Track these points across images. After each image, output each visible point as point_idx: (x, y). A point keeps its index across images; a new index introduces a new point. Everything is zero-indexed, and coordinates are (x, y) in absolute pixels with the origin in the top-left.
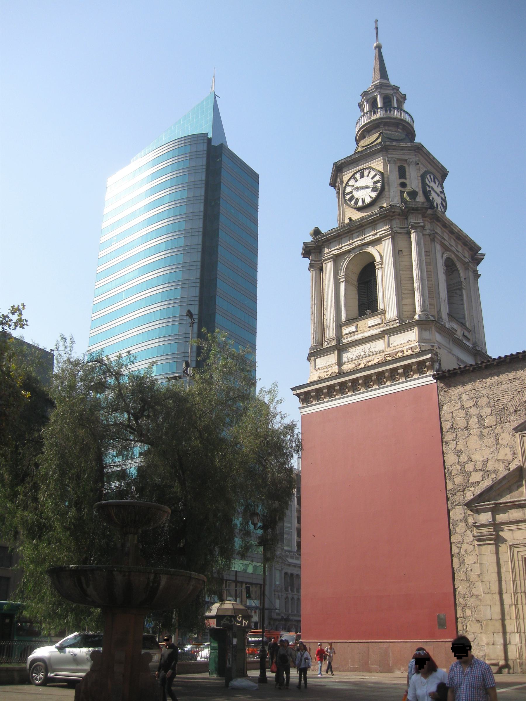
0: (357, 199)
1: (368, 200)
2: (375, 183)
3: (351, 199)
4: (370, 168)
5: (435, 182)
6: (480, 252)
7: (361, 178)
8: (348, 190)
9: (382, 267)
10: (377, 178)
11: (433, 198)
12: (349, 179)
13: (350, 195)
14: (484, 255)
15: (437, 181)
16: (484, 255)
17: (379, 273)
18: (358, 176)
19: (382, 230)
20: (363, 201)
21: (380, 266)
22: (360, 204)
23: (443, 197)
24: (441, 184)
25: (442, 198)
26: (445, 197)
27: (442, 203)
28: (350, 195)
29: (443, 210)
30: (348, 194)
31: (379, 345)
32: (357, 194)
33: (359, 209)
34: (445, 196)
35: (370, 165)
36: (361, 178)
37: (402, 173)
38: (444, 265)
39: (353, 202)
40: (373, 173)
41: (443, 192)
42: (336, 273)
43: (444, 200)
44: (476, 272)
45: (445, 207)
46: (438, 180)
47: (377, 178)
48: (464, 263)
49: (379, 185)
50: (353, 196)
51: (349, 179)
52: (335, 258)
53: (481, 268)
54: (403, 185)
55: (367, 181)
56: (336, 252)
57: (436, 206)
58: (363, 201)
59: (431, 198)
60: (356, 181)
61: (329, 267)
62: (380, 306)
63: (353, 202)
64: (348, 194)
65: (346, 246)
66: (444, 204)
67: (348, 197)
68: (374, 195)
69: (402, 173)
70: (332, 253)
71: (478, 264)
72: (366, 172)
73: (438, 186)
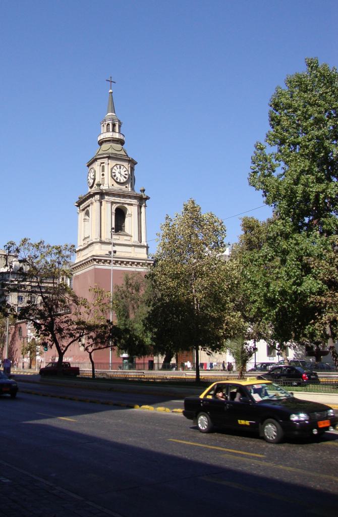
1: (122, 181)
2: (126, 174)
8: (113, 171)
18: (118, 166)
22: (118, 181)
30: (113, 173)
33: (117, 182)
39: (115, 178)
40: (125, 169)
47: (126, 173)
56: (113, 200)
63: (115, 178)
65: (117, 200)
67: (113, 174)
68: (125, 180)
72: (122, 167)
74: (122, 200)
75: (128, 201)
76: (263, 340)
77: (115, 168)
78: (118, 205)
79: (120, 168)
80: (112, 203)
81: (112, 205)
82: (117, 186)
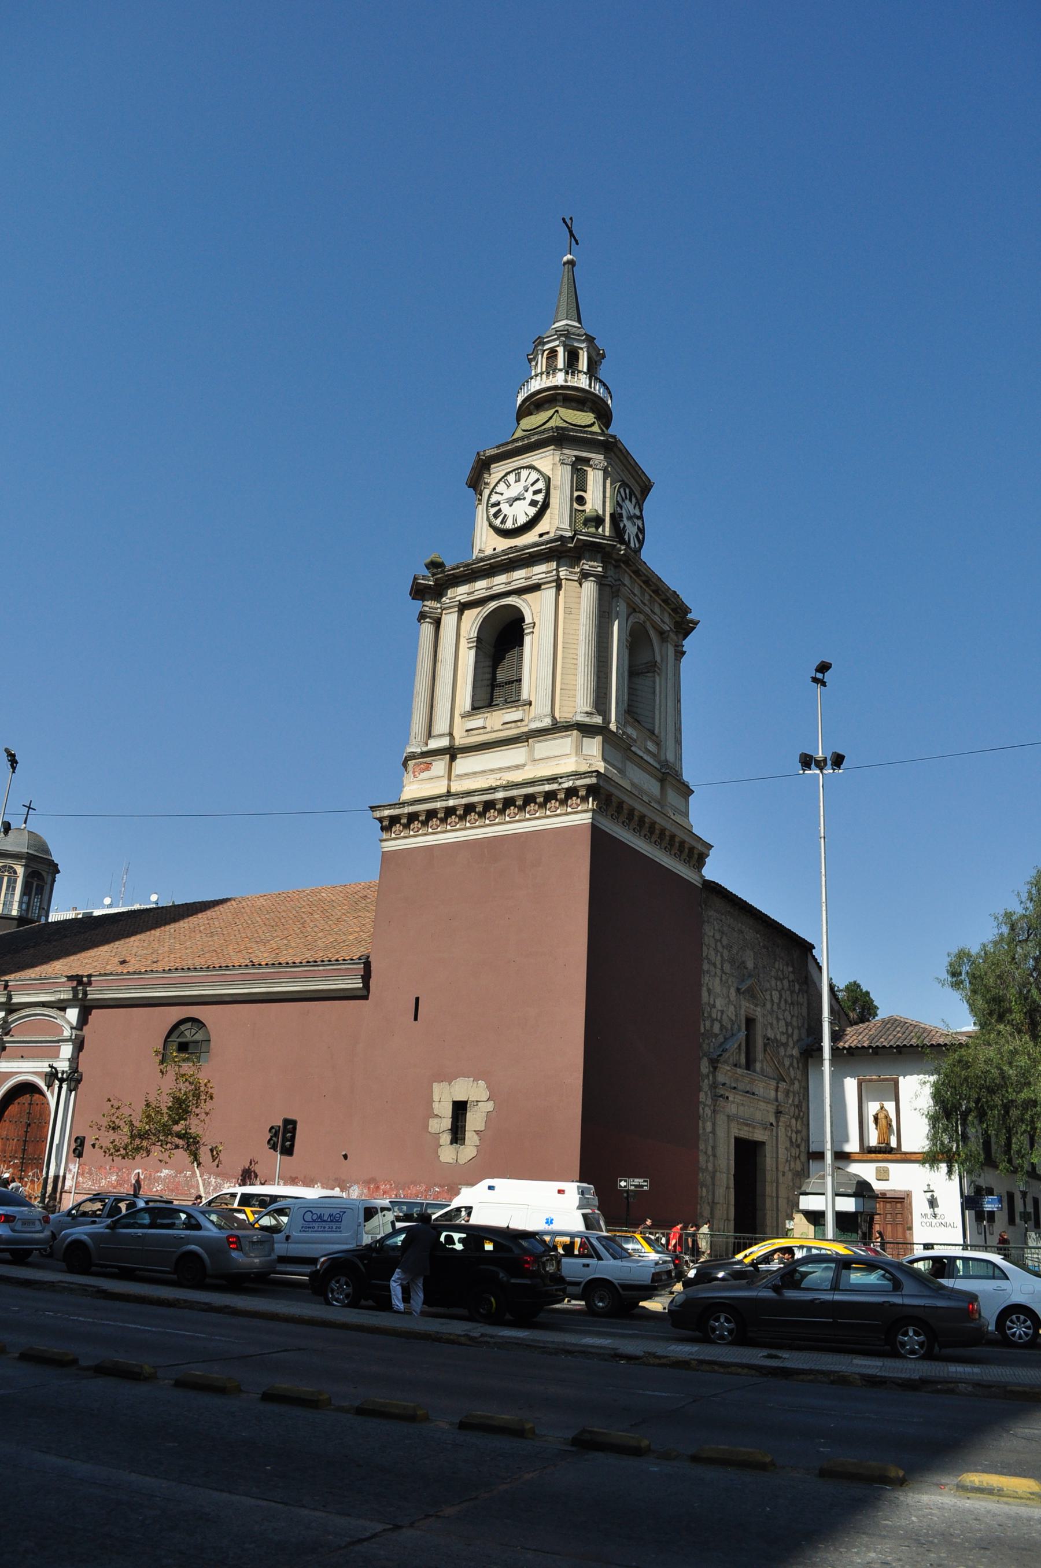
0: (505, 515)
1: (522, 520)
2: (535, 493)
4: (531, 467)
5: (631, 500)
6: (690, 616)
7: (516, 482)
9: (533, 632)
10: (541, 485)
11: (625, 526)
12: (498, 482)
13: (497, 508)
14: (696, 623)
15: (634, 500)
16: (696, 623)
17: (527, 640)
19: (540, 571)
20: (515, 520)
21: (531, 630)
22: (509, 525)
23: (641, 526)
24: (640, 505)
25: (638, 527)
26: (644, 527)
27: (637, 535)
28: (497, 508)
29: (637, 546)
31: (515, 755)
32: (505, 508)
34: (643, 524)
35: (534, 463)
36: (516, 482)
37: (580, 483)
38: (628, 634)
41: (641, 517)
43: (641, 530)
44: (680, 648)
45: (641, 543)
46: (636, 497)
47: (541, 485)
48: (662, 634)
49: (540, 498)
50: (500, 511)
51: (498, 482)
52: (461, 606)
53: (688, 644)
54: (581, 500)
56: (464, 599)
57: (627, 539)
58: (515, 520)
59: (622, 525)
61: (449, 620)
64: (493, 505)
66: (641, 537)
67: (493, 511)
68: (532, 511)
69: (580, 483)
70: (457, 599)
71: (686, 635)
72: (524, 473)
73: (634, 508)
74: (500, 582)
75: (519, 577)
76: (441, 1158)
77: (502, 487)
78: (493, 605)
80: (463, 607)
81: (461, 612)
82: (503, 544)
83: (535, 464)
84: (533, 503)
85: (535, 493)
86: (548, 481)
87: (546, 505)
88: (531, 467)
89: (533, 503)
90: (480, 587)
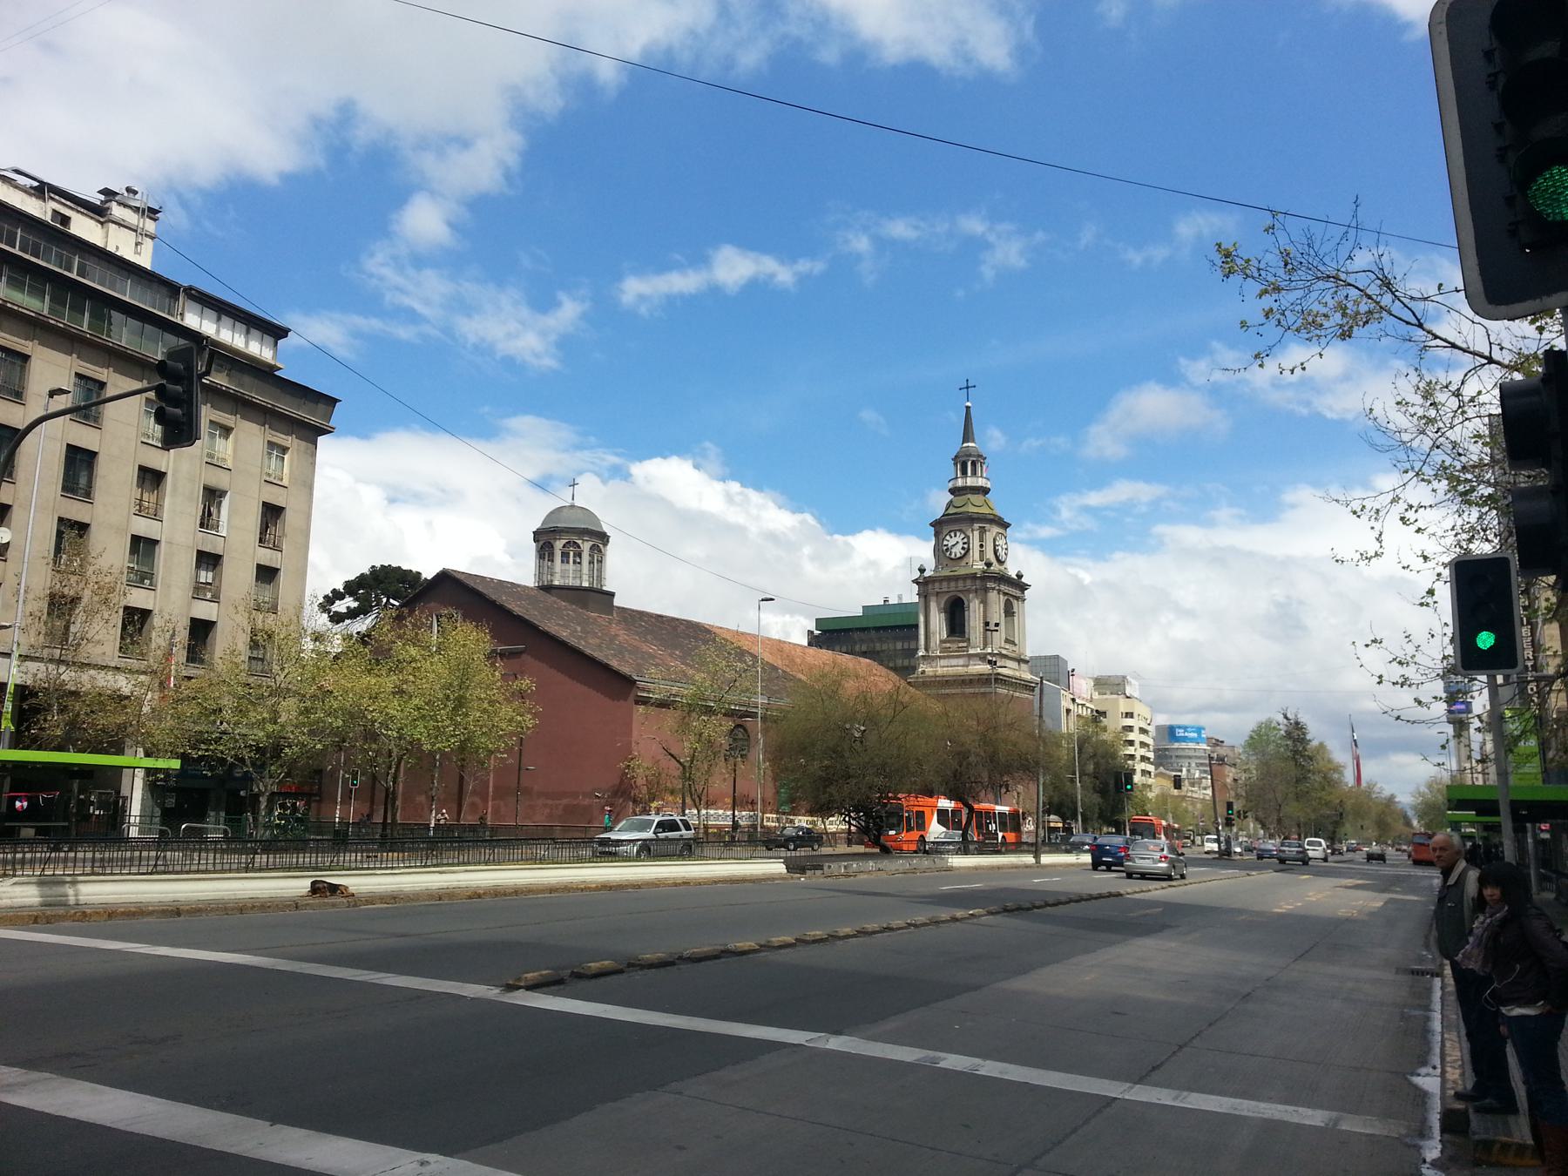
1: (958, 555)
2: (964, 543)
3: (947, 550)
17: (966, 613)
18: (952, 534)
20: (956, 555)
40: (963, 536)
42: (938, 605)
47: (965, 540)
55: (959, 537)
58: (956, 555)
60: (951, 537)
62: (967, 636)
67: (945, 548)
68: (963, 552)
72: (958, 534)
77: (948, 538)
79: (955, 536)
83: (964, 529)
84: (963, 548)
85: (964, 543)
86: (968, 538)
87: (969, 549)
88: (959, 530)
89: (963, 548)
90: (945, 584)
